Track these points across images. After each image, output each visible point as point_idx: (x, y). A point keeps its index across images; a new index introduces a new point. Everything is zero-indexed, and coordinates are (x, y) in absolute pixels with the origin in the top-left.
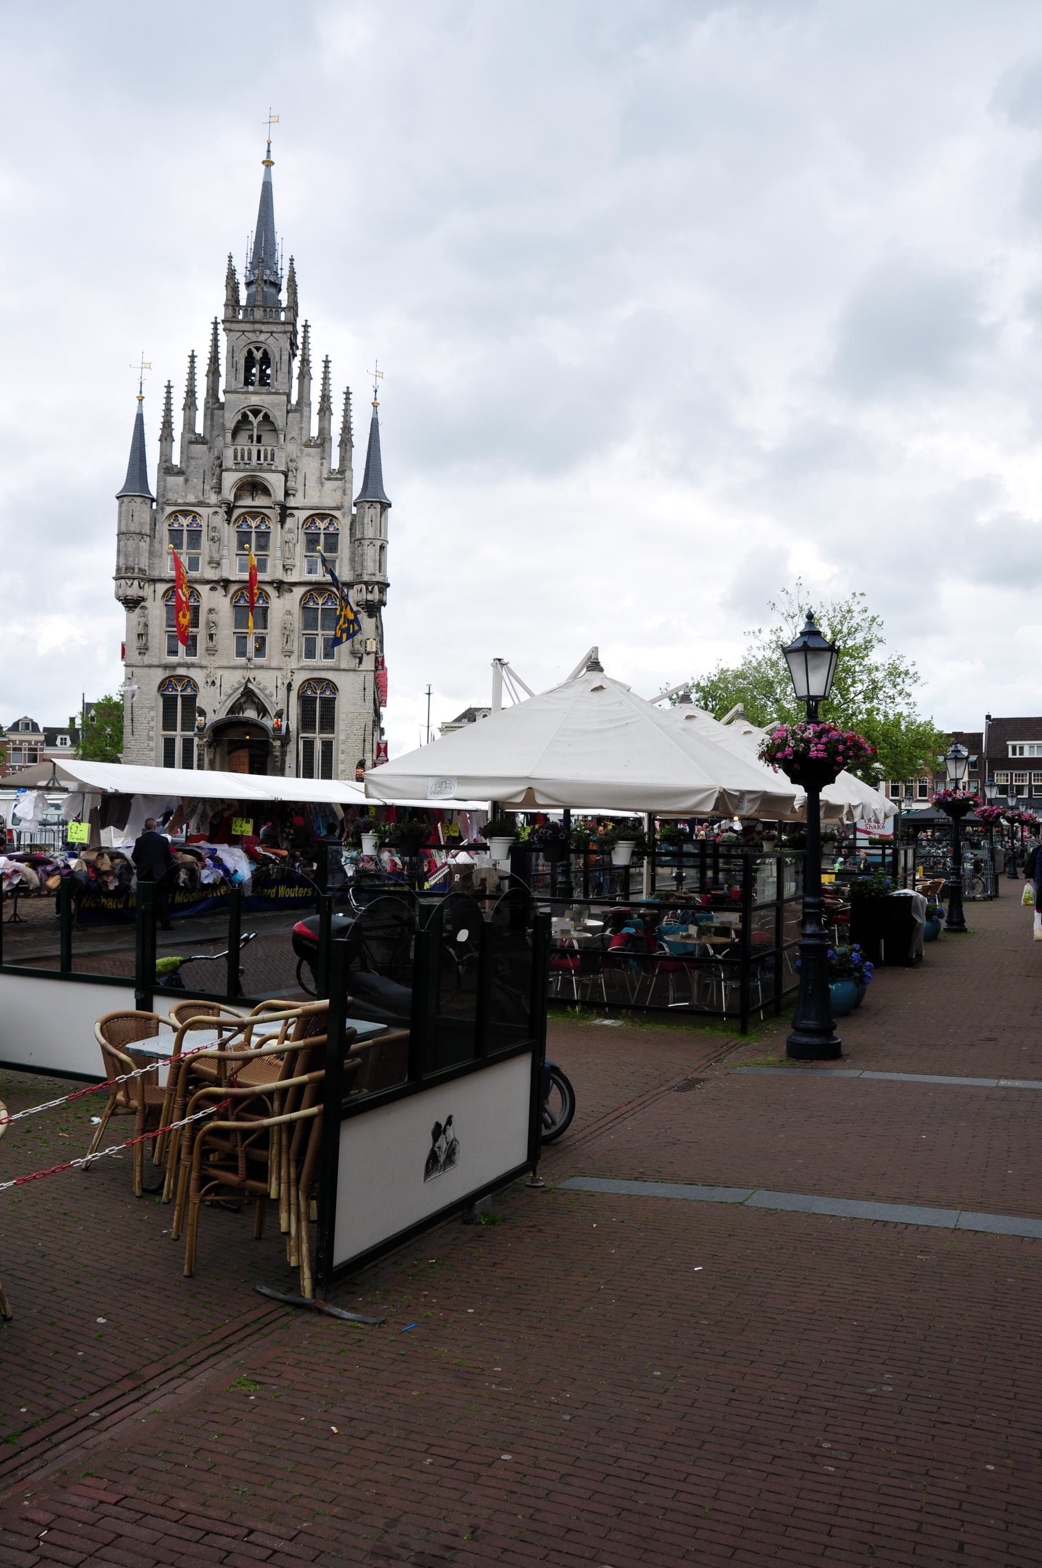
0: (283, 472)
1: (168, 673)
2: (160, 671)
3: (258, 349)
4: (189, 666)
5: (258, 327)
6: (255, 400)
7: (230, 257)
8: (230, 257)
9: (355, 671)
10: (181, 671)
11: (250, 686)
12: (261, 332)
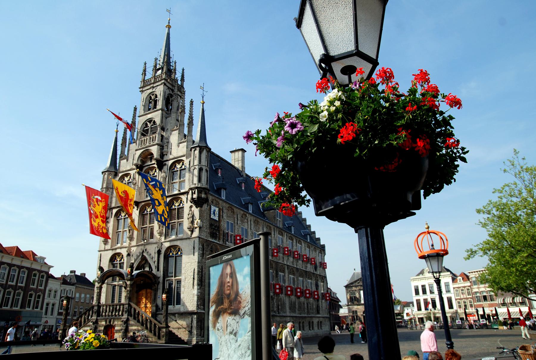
0: (158, 144)
1: (114, 252)
2: (111, 251)
3: (153, 95)
4: (121, 248)
5: (152, 85)
6: (149, 116)
7: (145, 64)
8: (145, 64)
9: (189, 238)
10: (118, 251)
11: (145, 254)
12: (153, 87)
